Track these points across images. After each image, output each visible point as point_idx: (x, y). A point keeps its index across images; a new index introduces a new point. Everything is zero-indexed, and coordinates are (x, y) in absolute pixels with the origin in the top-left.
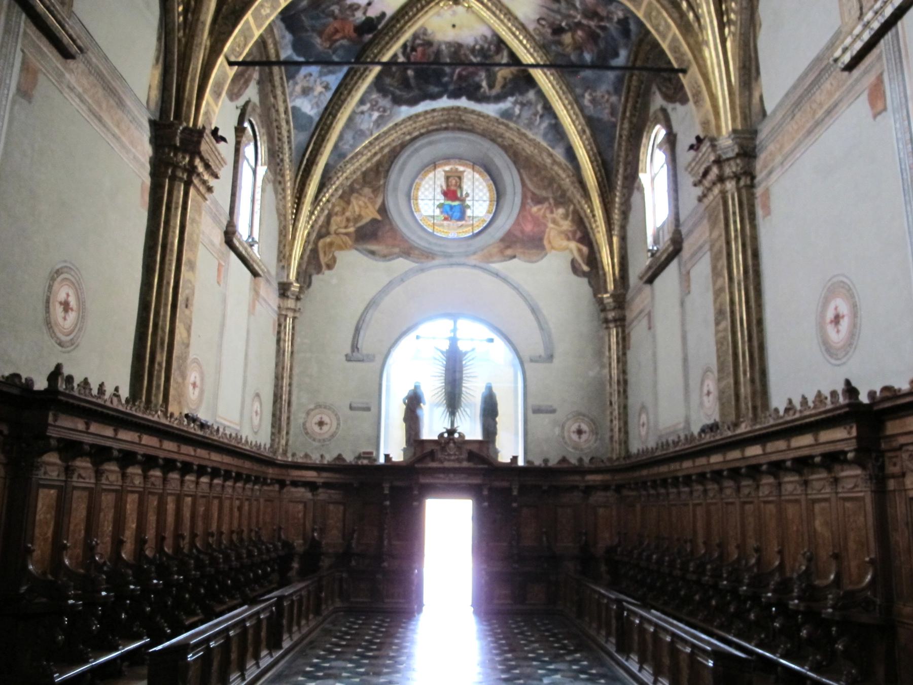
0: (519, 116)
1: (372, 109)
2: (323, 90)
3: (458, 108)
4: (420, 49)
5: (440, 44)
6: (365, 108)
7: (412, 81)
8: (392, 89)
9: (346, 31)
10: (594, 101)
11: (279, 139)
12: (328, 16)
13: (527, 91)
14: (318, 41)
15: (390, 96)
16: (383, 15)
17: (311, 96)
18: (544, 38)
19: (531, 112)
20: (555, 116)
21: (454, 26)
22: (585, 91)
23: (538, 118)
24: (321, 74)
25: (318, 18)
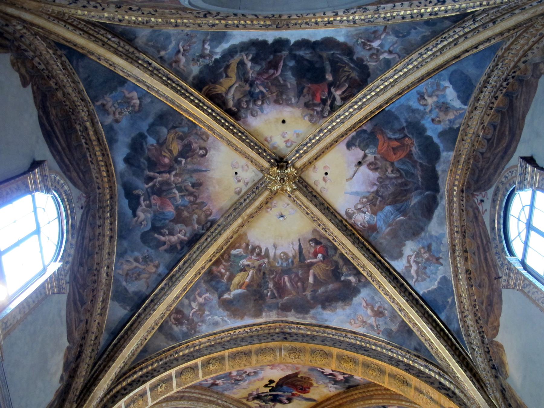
0: (204, 42)
1: (378, 52)
2: (426, 97)
3: (278, 28)
4: (317, 101)
5: (297, 105)
6: (386, 56)
7: (328, 68)
8: (352, 65)
9: (386, 145)
10: (127, 102)
11: (496, 98)
12: (398, 170)
13: (201, 72)
14: (415, 150)
15: (355, 58)
16: (349, 145)
17: (442, 100)
18: (196, 134)
19: (191, 52)
20: (162, 60)
21: (284, 122)
22: (140, 105)
23: (182, 50)
24: (423, 114)
25: (407, 172)
